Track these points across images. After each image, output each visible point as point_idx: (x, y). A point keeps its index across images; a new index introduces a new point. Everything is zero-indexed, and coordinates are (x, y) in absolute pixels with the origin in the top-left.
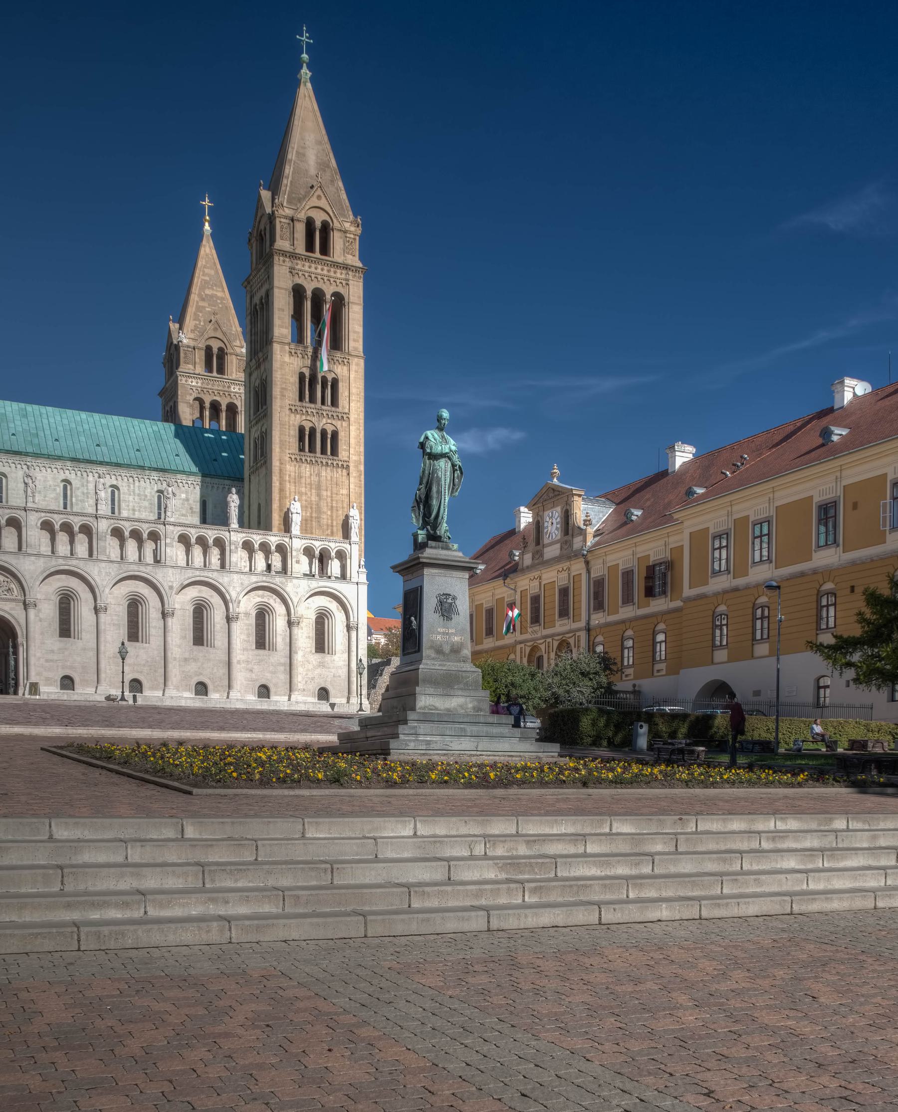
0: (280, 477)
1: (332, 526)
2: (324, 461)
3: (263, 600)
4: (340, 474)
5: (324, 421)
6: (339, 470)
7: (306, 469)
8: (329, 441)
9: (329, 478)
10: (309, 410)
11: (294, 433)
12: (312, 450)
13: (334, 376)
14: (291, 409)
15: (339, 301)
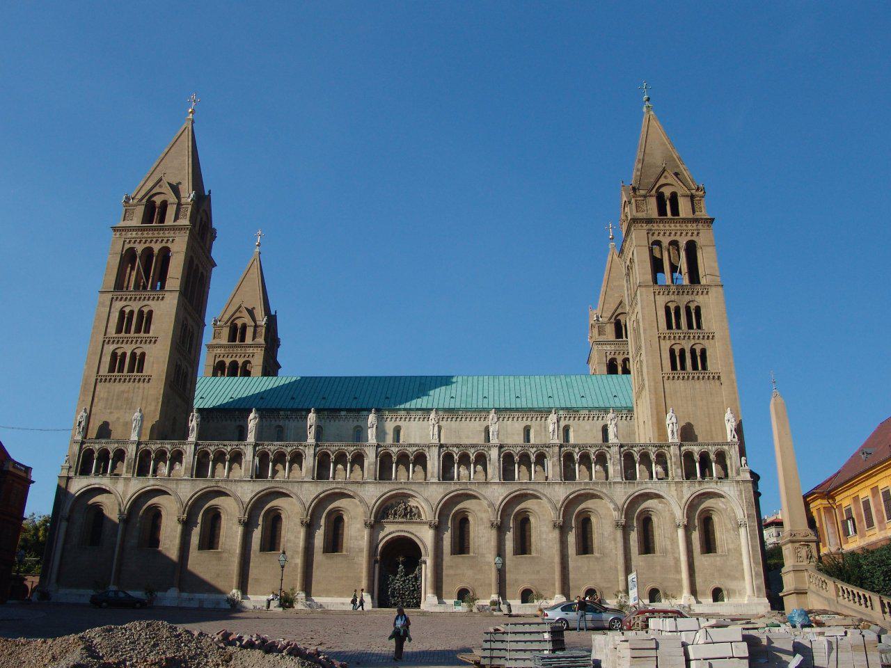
0: (656, 394)
1: (711, 431)
4: (714, 384)
5: (693, 342)
8: (699, 358)
10: (677, 336)
12: (683, 368)
13: (696, 304)
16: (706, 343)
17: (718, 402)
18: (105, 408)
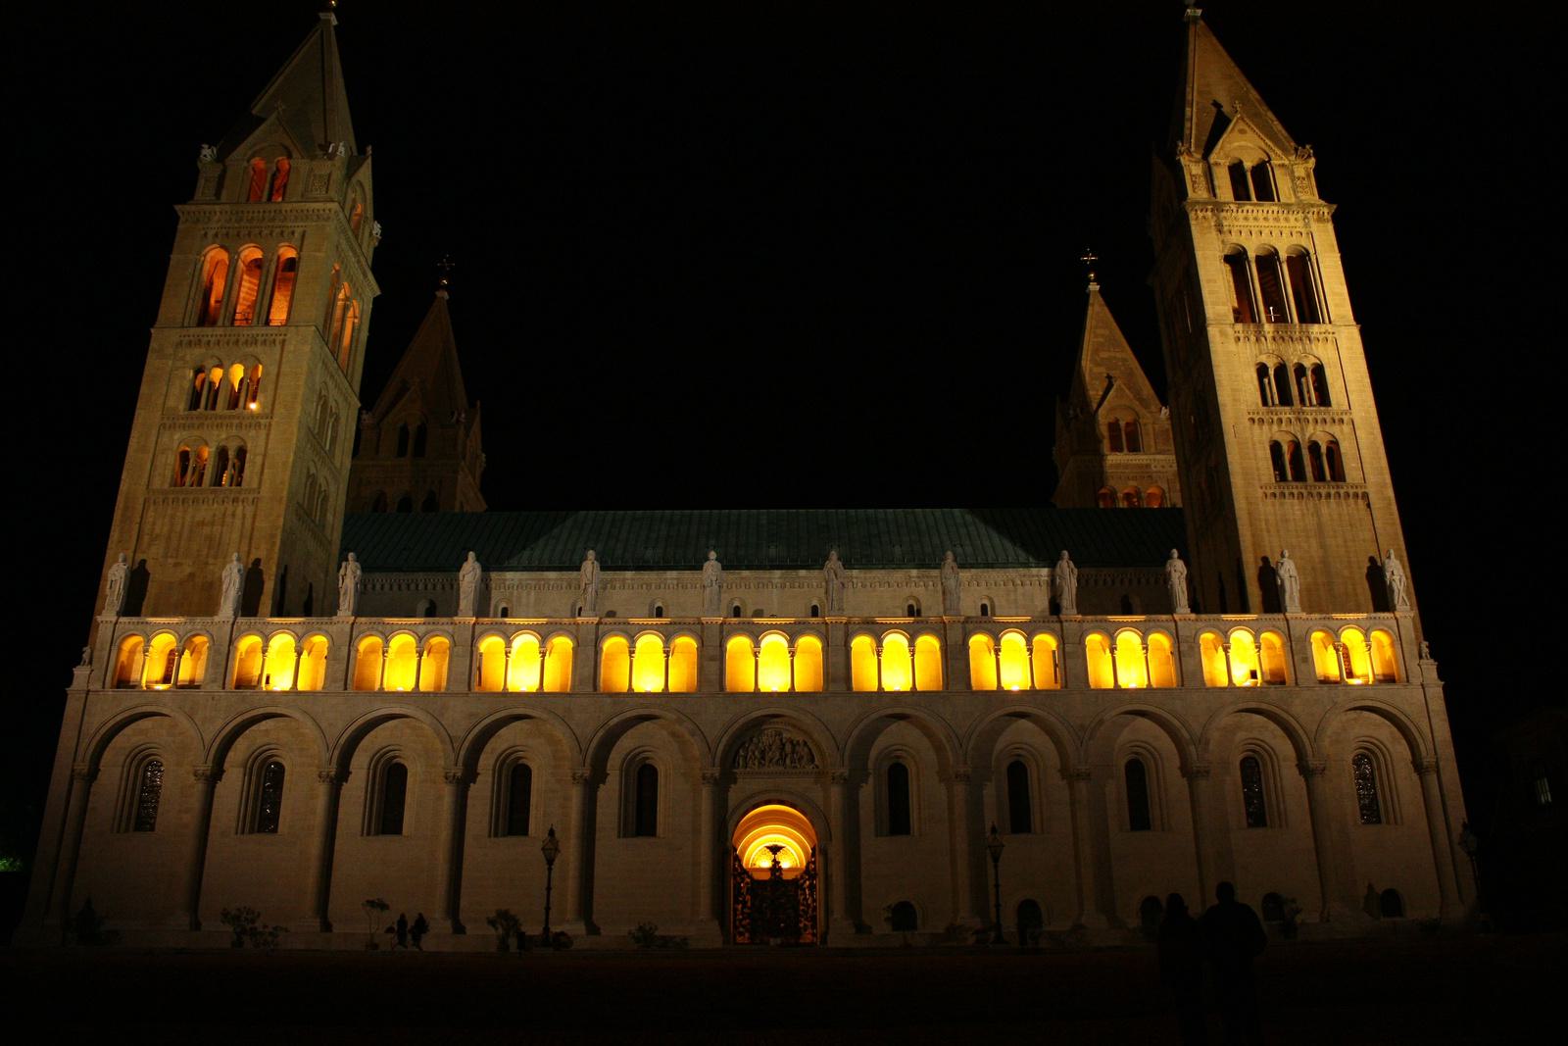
1: (1356, 595)
2: (1323, 492)
3: (1251, 736)
6: (1351, 500)
7: (1294, 508)
9: (1335, 517)
11: (1265, 455)
12: (1299, 476)
14: (1253, 420)
15: (1301, 262)
16: (1342, 433)
17: (1364, 541)
18: (166, 556)
